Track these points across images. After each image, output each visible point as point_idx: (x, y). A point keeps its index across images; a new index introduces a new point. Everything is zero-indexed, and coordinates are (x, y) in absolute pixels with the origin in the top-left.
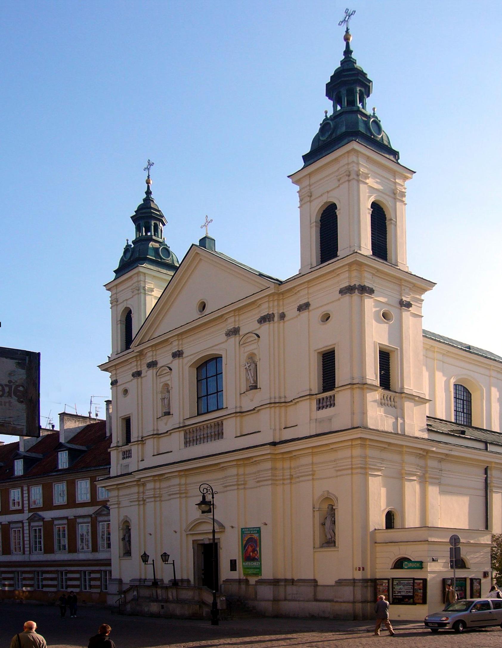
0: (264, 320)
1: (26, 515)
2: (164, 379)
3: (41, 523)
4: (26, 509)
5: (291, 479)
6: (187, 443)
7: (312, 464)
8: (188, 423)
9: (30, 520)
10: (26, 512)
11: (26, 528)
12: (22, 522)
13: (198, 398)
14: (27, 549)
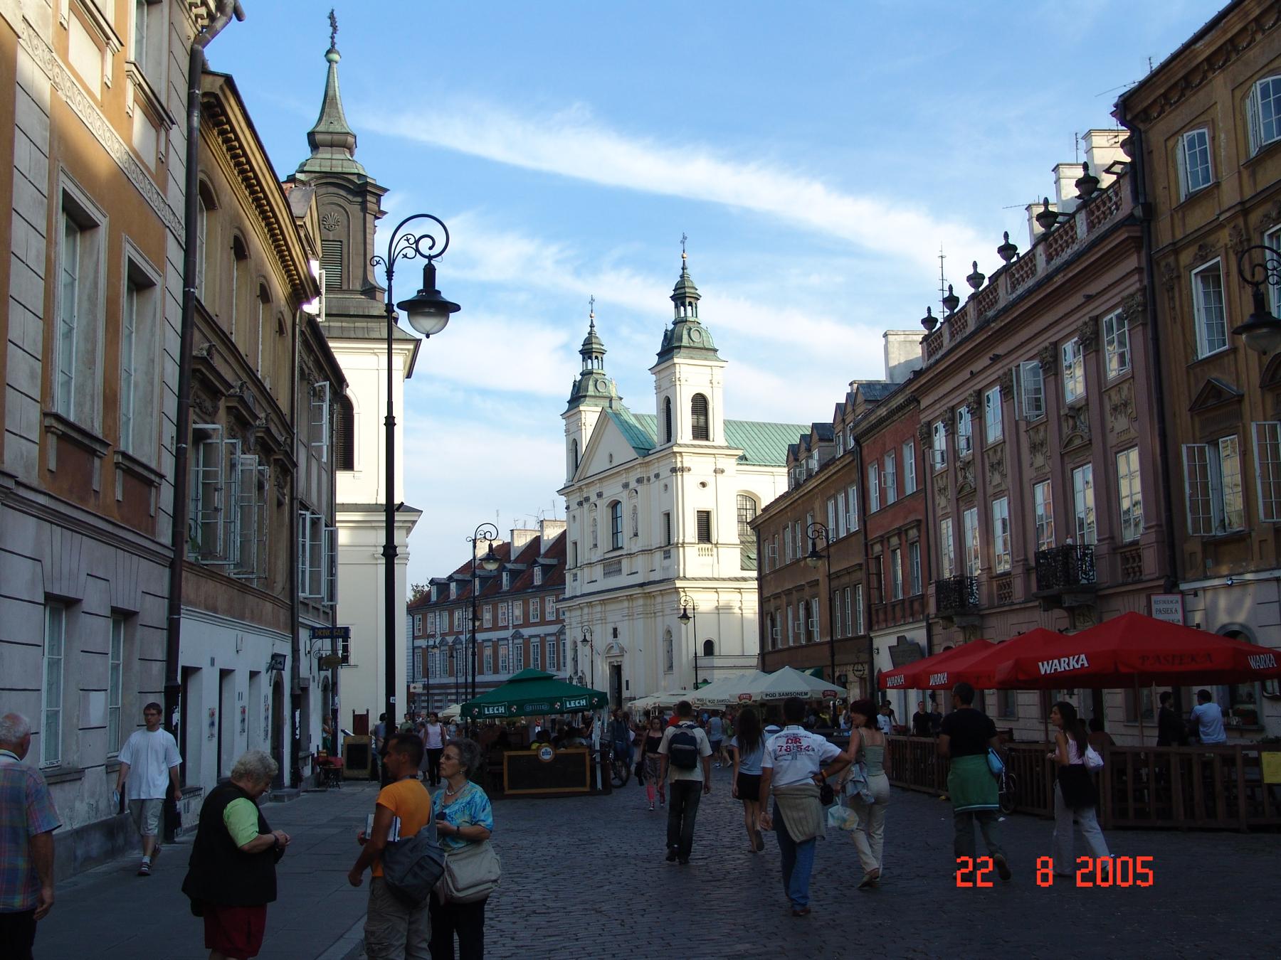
0: (639, 481)
1: (511, 632)
2: (594, 514)
3: (521, 641)
4: (511, 625)
5: (655, 613)
6: (607, 574)
7: (662, 603)
8: (608, 556)
9: (514, 637)
10: (511, 628)
11: (511, 645)
12: (506, 639)
13: (613, 534)
14: (511, 668)
